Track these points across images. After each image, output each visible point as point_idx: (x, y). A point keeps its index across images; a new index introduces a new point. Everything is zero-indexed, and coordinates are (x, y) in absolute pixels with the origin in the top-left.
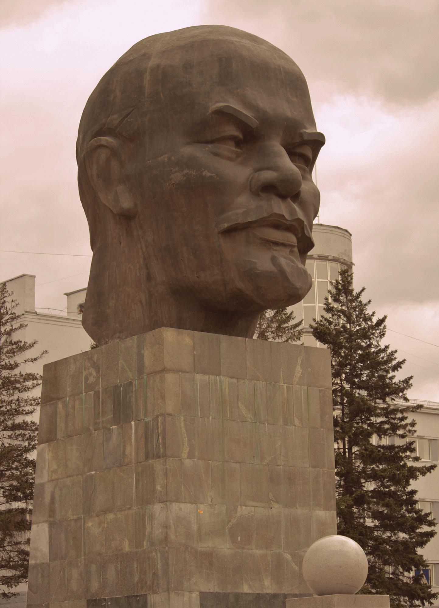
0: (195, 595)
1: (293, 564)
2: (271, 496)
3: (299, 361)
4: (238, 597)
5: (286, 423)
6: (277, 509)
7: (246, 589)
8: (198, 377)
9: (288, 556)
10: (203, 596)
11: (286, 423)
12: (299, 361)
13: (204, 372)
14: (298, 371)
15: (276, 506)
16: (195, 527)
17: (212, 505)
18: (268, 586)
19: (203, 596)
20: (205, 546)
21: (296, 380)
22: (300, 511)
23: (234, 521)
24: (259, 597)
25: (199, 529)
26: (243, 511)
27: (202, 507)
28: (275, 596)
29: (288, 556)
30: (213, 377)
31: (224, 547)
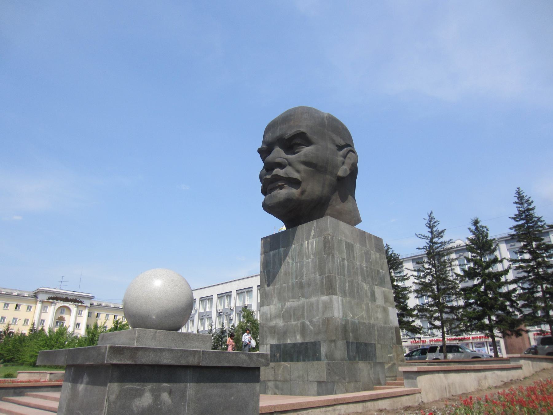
0: (268, 346)
1: (310, 327)
2: (300, 295)
3: (313, 228)
4: (285, 345)
5: (307, 259)
6: (302, 300)
7: (289, 341)
8: (272, 253)
9: (308, 323)
10: (272, 346)
11: (307, 259)
12: (313, 228)
13: (274, 250)
14: (313, 232)
15: (302, 299)
16: (269, 316)
17: (275, 305)
18: (299, 339)
19: (272, 346)
20: (273, 323)
21: (311, 237)
22: (313, 299)
23: (284, 310)
24: (295, 345)
25: (271, 316)
26: (288, 304)
27: (272, 306)
28: (302, 344)
29: (308, 323)
30: (277, 251)
31: (280, 323)
